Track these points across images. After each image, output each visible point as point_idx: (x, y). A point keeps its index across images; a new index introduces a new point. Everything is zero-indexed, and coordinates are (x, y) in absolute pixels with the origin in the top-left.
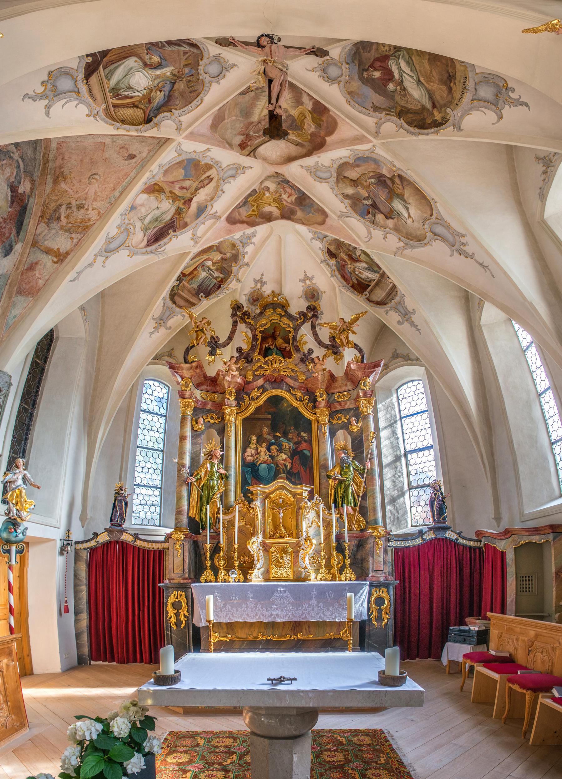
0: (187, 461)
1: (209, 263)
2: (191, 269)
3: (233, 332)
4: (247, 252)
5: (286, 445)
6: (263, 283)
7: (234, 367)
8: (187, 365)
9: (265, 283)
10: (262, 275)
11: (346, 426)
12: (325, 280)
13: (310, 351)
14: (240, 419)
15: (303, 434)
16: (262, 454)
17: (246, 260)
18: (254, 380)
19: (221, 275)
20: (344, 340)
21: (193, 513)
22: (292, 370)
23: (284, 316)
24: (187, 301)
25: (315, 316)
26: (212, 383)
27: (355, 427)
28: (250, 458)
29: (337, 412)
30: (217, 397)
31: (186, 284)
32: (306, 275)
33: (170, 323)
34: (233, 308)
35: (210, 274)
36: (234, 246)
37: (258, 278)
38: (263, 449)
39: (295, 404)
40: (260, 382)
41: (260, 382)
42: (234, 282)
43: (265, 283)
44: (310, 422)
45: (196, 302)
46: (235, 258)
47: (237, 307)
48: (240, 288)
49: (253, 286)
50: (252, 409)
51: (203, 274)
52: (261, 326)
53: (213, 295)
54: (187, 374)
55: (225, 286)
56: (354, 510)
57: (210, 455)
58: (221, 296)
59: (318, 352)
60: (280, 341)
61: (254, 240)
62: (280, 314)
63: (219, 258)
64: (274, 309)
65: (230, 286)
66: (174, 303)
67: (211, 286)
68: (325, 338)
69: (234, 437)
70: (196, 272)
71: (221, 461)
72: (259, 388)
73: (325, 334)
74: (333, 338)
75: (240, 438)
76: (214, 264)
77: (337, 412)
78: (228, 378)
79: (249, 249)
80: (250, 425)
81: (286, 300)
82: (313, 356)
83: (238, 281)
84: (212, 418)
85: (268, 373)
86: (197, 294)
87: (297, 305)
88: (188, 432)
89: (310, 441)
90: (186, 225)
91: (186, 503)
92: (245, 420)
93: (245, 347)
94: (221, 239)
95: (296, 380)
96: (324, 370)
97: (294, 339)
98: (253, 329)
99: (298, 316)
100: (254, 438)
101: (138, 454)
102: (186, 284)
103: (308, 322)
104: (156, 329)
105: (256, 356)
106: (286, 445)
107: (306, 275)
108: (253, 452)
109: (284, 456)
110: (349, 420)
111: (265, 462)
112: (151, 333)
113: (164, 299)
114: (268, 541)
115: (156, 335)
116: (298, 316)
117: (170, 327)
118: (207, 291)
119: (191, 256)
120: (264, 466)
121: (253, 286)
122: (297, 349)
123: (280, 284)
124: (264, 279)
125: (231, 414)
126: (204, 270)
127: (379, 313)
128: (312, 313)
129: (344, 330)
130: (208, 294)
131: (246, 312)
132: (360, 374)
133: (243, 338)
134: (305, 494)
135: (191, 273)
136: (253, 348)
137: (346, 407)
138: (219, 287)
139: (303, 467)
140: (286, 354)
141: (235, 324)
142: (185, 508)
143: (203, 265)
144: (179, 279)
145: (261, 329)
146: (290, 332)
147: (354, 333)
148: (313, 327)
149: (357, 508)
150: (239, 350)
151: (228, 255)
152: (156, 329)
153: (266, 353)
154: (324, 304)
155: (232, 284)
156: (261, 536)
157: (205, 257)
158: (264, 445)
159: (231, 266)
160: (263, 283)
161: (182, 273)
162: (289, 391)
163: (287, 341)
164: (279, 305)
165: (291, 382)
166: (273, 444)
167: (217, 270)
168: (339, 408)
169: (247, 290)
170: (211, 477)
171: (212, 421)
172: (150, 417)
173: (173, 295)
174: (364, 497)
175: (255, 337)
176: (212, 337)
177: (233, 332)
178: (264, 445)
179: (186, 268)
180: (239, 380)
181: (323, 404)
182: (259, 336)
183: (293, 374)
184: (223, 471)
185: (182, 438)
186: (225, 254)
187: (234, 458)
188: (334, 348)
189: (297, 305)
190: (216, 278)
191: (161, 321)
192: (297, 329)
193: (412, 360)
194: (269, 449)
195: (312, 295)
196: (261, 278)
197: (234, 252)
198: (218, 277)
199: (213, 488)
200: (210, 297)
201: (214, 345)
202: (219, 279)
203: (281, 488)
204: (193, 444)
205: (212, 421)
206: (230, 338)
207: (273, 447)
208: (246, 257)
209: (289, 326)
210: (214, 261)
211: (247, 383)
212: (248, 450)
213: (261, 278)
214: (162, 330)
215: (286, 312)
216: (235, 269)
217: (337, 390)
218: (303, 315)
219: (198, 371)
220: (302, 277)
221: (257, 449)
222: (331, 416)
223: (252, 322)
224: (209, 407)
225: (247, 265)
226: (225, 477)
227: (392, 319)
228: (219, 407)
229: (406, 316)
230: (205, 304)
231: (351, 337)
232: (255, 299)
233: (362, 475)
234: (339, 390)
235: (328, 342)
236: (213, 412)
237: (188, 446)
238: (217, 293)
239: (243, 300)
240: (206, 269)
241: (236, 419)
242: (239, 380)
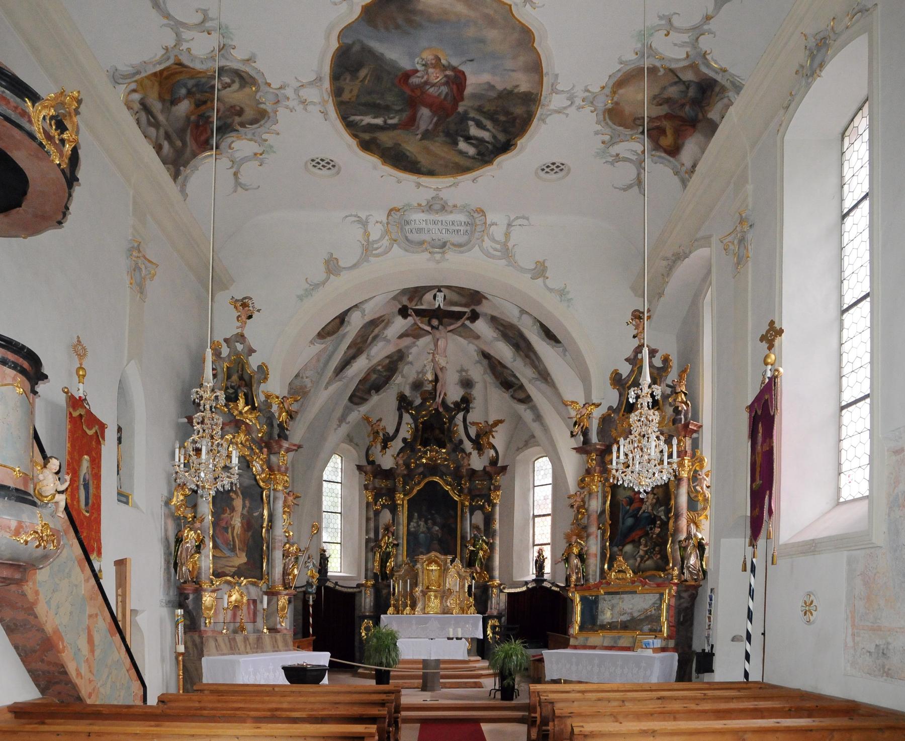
0: (372, 535)
1: (380, 368)
3: (399, 424)
5: (439, 520)
11: (482, 508)
12: (478, 373)
14: (405, 502)
15: (452, 512)
25: (467, 410)
30: (389, 483)
38: (422, 523)
39: (447, 488)
41: (421, 469)
47: (402, 398)
50: (415, 491)
57: (387, 529)
59: (468, 445)
60: (437, 432)
69: (403, 516)
71: (393, 535)
72: (420, 474)
74: (478, 435)
88: (372, 514)
93: (408, 436)
95: (448, 466)
97: (449, 428)
99: (452, 406)
104: (339, 426)
106: (439, 520)
109: (437, 528)
111: (423, 532)
116: (452, 406)
120: (422, 535)
122: (451, 441)
127: (521, 408)
128: (465, 404)
133: (406, 432)
134: (449, 561)
136: (415, 437)
139: (447, 543)
141: (401, 417)
146: (445, 423)
147: (493, 437)
150: (404, 440)
153: (425, 443)
154: (477, 392)
155: (398, 379)
162: (441, 477)
163: (442, 431)
165: (444, 469)
168: (478, 493)
175: (416, 426)
176: (384, 435)
177: (399, 424)
181: (466, 491)
184: (395, 542)
187: (403, 530)
189: (454, 394)
191: (342, 419)
194: (426, 522)
195: (467, 384)
201: (387, 441)
206: (397, 430)
218: (456, 404)
221: (417, 523)
222: (472, 499)
225: (411, 363)
227: (528, 416)
228: (391, 493)
229: (538, 417)
230: (375, 399)
231: (492, 440)
239: (407, 392)
242: (405, 472)
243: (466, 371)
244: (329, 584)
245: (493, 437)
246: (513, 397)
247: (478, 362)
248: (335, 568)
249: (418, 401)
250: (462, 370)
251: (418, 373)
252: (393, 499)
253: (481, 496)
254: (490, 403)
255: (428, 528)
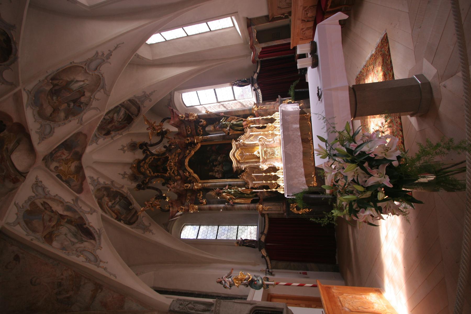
0: (222, 206)
1: (110, 204)
2: (113, 214)
4: (104, 182)
5: (213, 157)
6: (125, 173)
7: (173, 185)
8: (171, 209)
9: (125, 172)
10: (119, 174)
11: (204, 127)
12: (123, 139)
13: (165, 147)
15: (208, 148)
16: (218, 169)
17: (108, 182)
18: (180, 175)
19: (118, 197)
20: (159, 127)
21: (249, 201)
22: (175, 156)
23: (145, 161)
24: (134, 215)
26: (181, 197)
27: (204, 122)
28: (220, 175)
29: (196, 132)
31: (123, 216)
32: (121, 149)
33: (147, 223)
34: (139, 189)
35: (118, 203)
36: (99, 190)
37: (122, 177)
38: (216, 169)
39: (193, 153)
40: (181, 172)
41: (181, 172)
42: (123, 189)
43: (125, 172)
44: (201, 146)
45: (135, 211)
46: (107, 189)
48: (127, 186)
49: (126, 179)
50: (196, 176)
51: (117, 207)
52: (150, 173)
53: (131, 201)
54: (176, 209)
55: (125, 194)
56: (245, 121)
58: (132, 196)
61: (95, 178)
62: (144, 163)
63: (107, 198)
64: (141, 167)
65: (126, 192)
66: (134, 222)
67: (126, 202)
68: (157, 139)
70: (116, 211)
71: (222, 189)
73: (155, 139)
74: (158, 134)
75: (210, 181)
76: (110, 201)
77: (196, 132)
78: (178, 187)
79: (102, 181)
80: (204, 176)
81: (136, 160)
82: (168, 145)
83: (123, 187)
84: (200, 196)
85: (176, 168)
86: (130, 210)
87: (139, 155)
89: (212, 146)
90: (81, 218)
91: (243, 205)
92: (201, 179)
94: (94, 196)
95: (179, 154)
96: (175, 138)
97: (157, 155)
98: (152, 178)
100: (210, 173)
101: (220, 238)
102: (123, 216)
103: (149, 149)
104: (150, 231)
105: (167, 175)
106: (213, 157)
107: (121, 149)
108: (217, 174)
109: (219, 158)
110: (200, 126)
111: (222, 168)
112: (153, 234)
113: (132, 228)
114: (261, 160)
115: (154, 231)
117: (150, 224)
118: (127, 204)
119: (104, 214)
120: (224, 168)
121: (126, 179)
122: (164, 153)
123: (125, 164)
124: (123, 173)
125: (198, 185)
126: (114, 207)
128: (144, 146)
129: (153, 128)
130: (130, 204)
131: (142, 182)
132: (177, 120)
133: (157, 183)
135: (116, 214)
136: (163, 177)
137: (194, 127)
138: (126, 198)
140: (167, 159)
142: (246, 205)
143: (111, 208)
144: (120, 220)
145: (152, 173)
146: (154, 158)
147: (155, 123)
148: (152, 145)
149: (244, 119)
150: (163, 184)
151: (105, 193)
152: (150, 231)
156: (258, 164)
157: (105, 206)
158: (213, 168)
159: (113, 191)
160: (125, 173)
161: (116, 219)
162: (186, 157)
164: (139, 164)
165: (181, 156)
166: (213, 164)
167: (115, 199)
169: (129, 183)
170: (230, 193)
171: (201, 195)
172: (200, 233)
173: (129, 223)
174: (239, 116)
178: (213, 168)
179: (112, 217)
180: (179, 182)
182: (156, 174)
183: (177, 155)
184: (227, 187)
185: (210, 209)
186: (104, 195)
188: (163, 134)
189: (139, 155)
190: (120, 200)
192: (152, 154)
193: (171, 98)
194: (216, 166)
195: (133, 147)
196: (122, 175)
197: (103, 190)
198: (119, 199)
199: (235, 191)
200: (132, 203)
202: (121, 198)
203: (234, 155)
204: (213, 204)
205: (201, 195)
207: (215, 164)
208: (107, 183)
209: (151, 158)
210: (108, 201)
211: (181, 179)
212: (216, 176)
213: (122, 175)
214: (151, 228)
215: (142, 160)
216: (115, 189)
217: (185, 133)
218: (144, 152)
219: (174, 203)
220: (122, 152)
221: (216, 172)
222: (198, 135)
223: (148, 179)
224: (194, 198)
226: (230, 186)
228: (194, 192)
231: (157, 124)
232: (134, 178)
233: (228, 118)
234: (185, 131)
235: (159, 138)
236: (197, 195)
237: (214, 206)
238: (129, 199)
239: (134, 185)
240: (114, 205)
241: (200, 183)
242: (179, 182)
243: (124, 147)
244: (263, 239)
245: (155, 123)
246: (136, 116)
247: (112, 138)
248: (249, 233)
249: (142, 176)
250: (123, 149)
251: (124, 177)
252: (199, 190)
253: (196, 128)
254: (140, 129)
255: (219, 165)
